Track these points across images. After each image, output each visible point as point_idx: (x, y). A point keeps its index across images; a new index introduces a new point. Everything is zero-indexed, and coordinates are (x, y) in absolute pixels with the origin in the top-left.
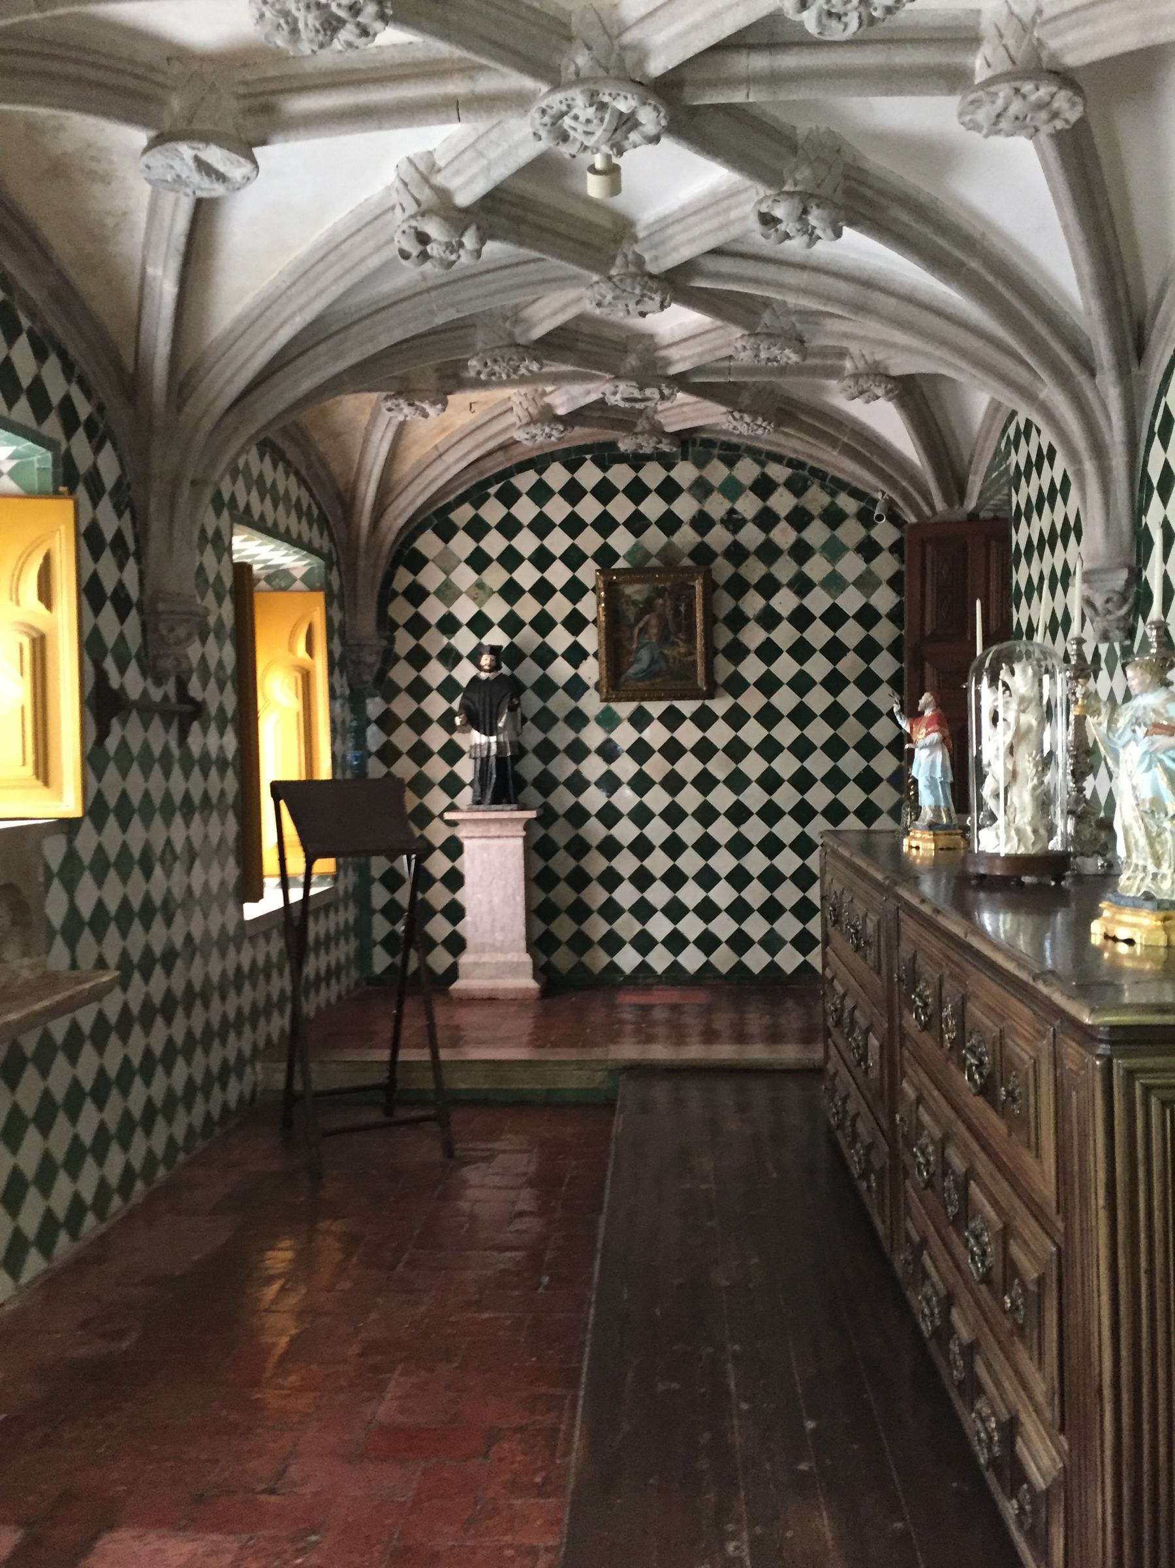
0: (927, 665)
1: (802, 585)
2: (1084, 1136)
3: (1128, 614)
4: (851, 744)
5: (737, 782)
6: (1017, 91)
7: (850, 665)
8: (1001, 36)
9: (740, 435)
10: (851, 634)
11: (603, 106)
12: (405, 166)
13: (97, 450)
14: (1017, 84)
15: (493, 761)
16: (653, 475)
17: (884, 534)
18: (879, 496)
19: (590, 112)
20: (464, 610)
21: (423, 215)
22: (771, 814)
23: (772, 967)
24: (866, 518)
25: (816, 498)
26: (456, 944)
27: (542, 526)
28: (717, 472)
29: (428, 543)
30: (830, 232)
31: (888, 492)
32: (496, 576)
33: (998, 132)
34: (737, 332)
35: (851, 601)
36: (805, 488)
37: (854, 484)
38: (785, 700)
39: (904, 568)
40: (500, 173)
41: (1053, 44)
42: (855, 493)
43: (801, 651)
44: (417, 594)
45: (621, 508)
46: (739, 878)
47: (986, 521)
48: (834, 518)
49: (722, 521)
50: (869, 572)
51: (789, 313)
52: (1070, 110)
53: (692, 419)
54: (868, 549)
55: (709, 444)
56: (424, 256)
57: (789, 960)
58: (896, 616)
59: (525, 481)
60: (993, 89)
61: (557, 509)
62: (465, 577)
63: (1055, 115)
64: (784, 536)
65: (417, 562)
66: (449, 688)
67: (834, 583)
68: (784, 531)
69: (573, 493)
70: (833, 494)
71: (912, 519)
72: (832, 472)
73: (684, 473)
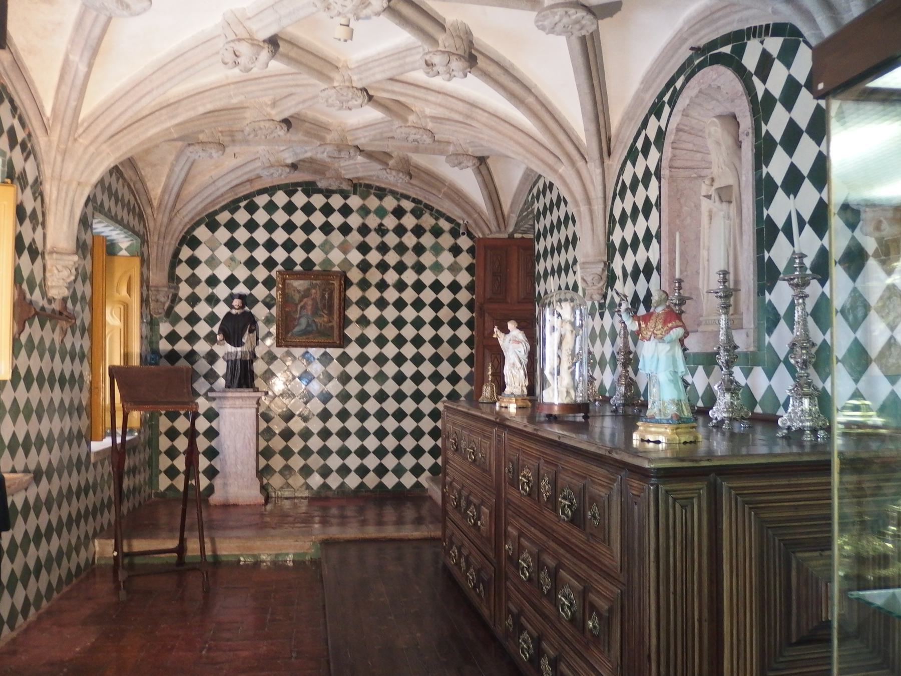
0: (487, 315)
1: (419, 268)
2: (642, 528)
4: (445, 357)
5: (381, 377)
7: (445, 314)
9: (390, 184)
10: (446, 296)
13: (26, 159)
14: (567, 9)
15: (239, 363)
17: (464, 242)
18: (461, 222)
20: (223, 273)
21: (239, 40)
22: (400, 397)
23: (399, 485)
24: (455, 233)
25: (428, 221)
26: (212, 473)
27: (271, 226)
28: (373, 202)
29: (202, 233)
30: (461, 74)
32: (242, 254)
33: (553, 33)
34: (397, 123)
35: (446, 278)
38: (409, 332)
39: (474, 261)
42: (449, 220)
43: (418, 305)
44: (193, 262)
45: (318, 219)
46: (381, 434)
48: (437, 232)
49: (375, 230)
50: (455, 262)
51: (426, 117)
54: (456, 250)
55: (369, 186)
57: (408, 480)
58: (471, 288)
59: (262, 200)
60: (555, 10)
61: (280, 217)
62: (223, 253)
64: (410, 240)
65: (194, 243)
66: (212, 319)
67: (437, 268)
68: (409, 237)
69: (290, 208)
70: (437, 219)
71: (481, 236)
72: (436, 207)
73: (355, 202)
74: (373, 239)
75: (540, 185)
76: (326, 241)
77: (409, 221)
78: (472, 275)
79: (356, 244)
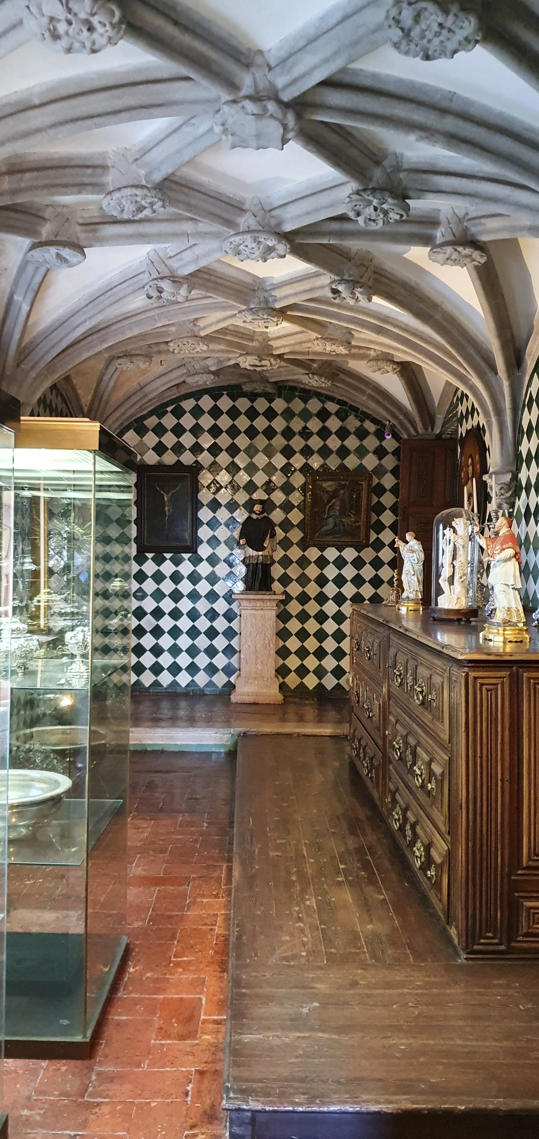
3: (511, 495)
6: (456, 250)
8: (449, 223)
11: (259, 242)
12: (152, 253)
16: (261, 405)
18: (387, 423)
19: (254, 245)
21: (162, 278)
24: (380, 435)
28: (297, 405)
31: (393, 421)
36: (347, 417)
37: (375, 416)
40: (202, 264)
41: (473, 230)
42: (374, 421)
45: (243, 423)
47: (445, 439)
48: (362, 434)
49: (300, 433)
50: (380, 465)
52: (480, 258)
53: (286, 375)
55: (293, 389)
56: (160, 297)
58: (395, 491)
59: (188, 405)
61: (206, 422)
63: (474, 260)
68: (333, 440)
69: (216, 412)
70: (362, 421)
72: (362, 408)
73: (279, 405)
74: (297, 443)
75: (459, 393)
76: (251, 444)
77: (334, 424)
78: (397, 477)
79: (280, 448)
